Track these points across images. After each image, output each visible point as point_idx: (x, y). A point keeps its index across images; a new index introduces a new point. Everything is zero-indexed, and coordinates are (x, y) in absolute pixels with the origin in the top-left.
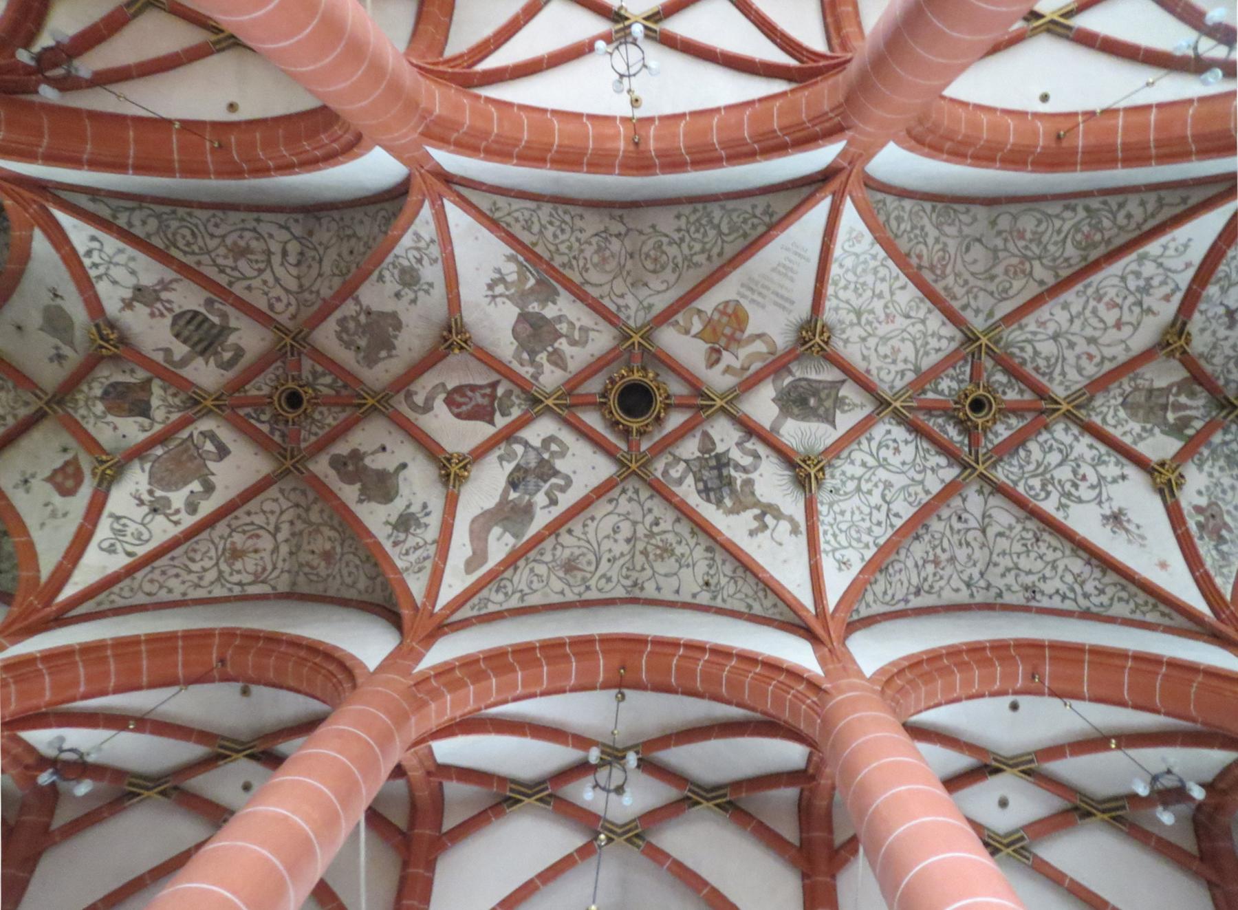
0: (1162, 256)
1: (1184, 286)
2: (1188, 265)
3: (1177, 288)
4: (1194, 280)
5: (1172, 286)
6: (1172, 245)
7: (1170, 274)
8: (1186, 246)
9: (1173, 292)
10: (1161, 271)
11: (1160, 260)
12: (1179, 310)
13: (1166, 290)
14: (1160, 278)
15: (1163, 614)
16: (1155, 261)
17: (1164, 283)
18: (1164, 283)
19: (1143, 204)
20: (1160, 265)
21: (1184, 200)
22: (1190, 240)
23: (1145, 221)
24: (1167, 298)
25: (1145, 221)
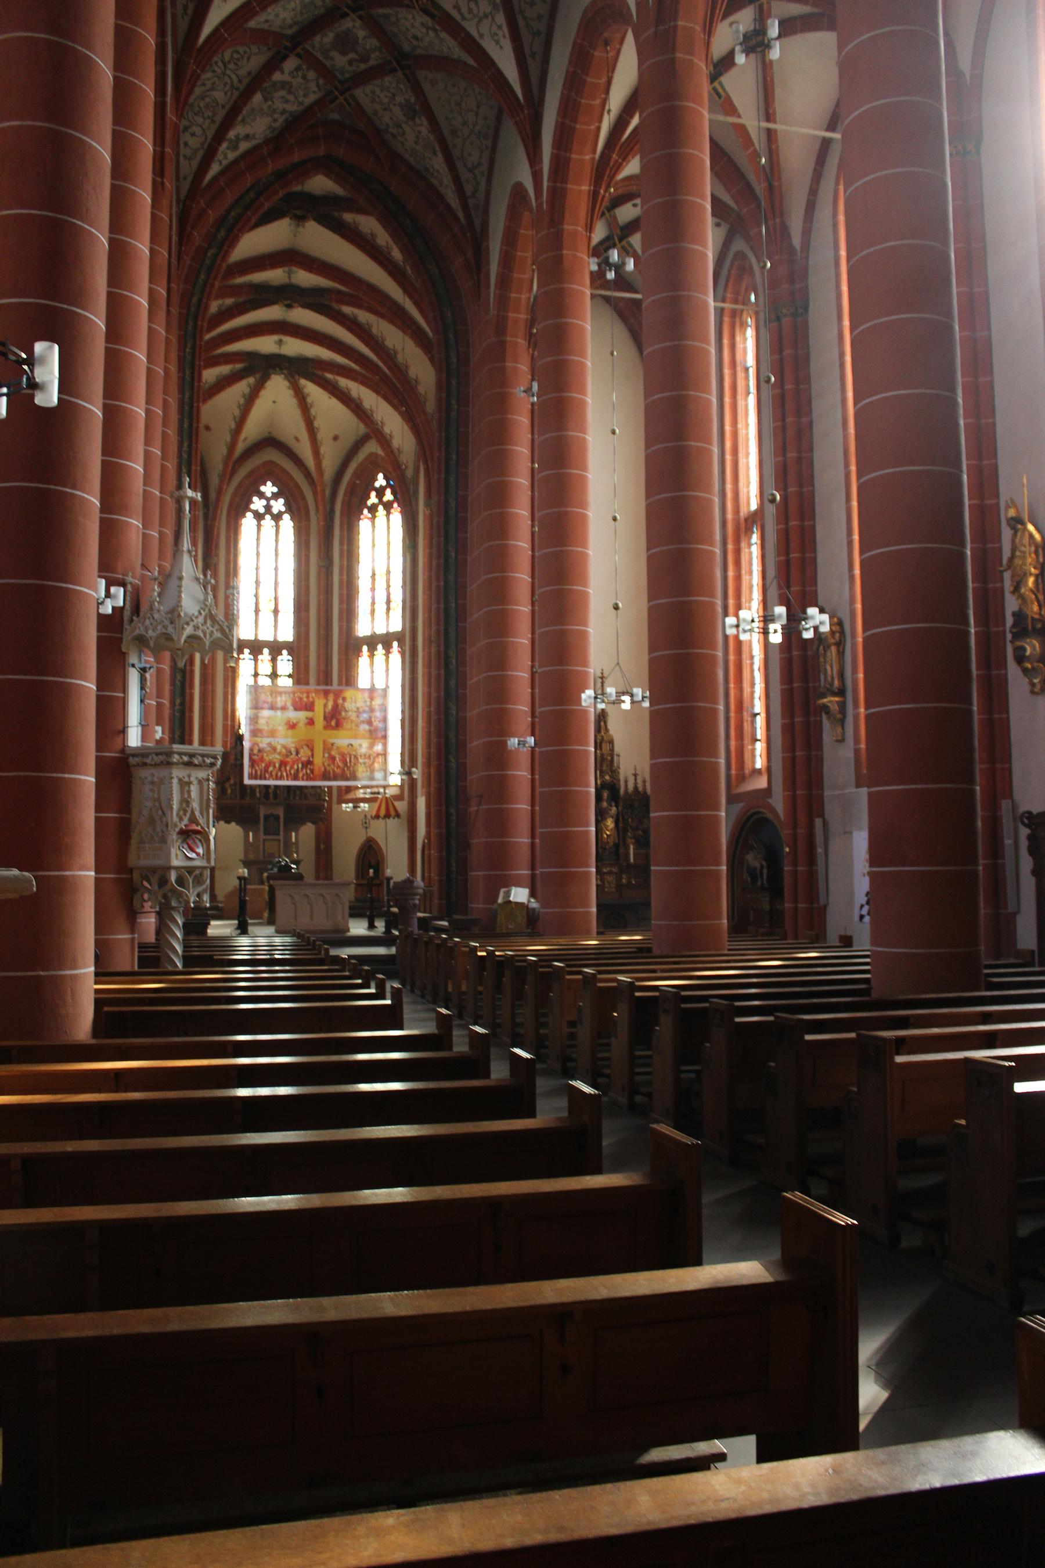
0: (493, 20)
1: (465, 24)
2: (481, 36)
3: (463, 18)
4: (468, 35)
5: (467, 15)
6: (500, 33)
7: (477, 19)
8: (497, 42)
9: (462, 15)
10: (481, 14)
11: (490, 19)
12: (447, 14)
13: (465, 10)
14: (475, 10)
15: (185, 7)
16: (491, 13)
17: (470, 11)
18: (470, 11)
19: (540, 17)
20: (486, 16)
21: (533, 55)
22: (501, 47)
23: (525, 18)
24: (457, 7)
25: (525, 18)
